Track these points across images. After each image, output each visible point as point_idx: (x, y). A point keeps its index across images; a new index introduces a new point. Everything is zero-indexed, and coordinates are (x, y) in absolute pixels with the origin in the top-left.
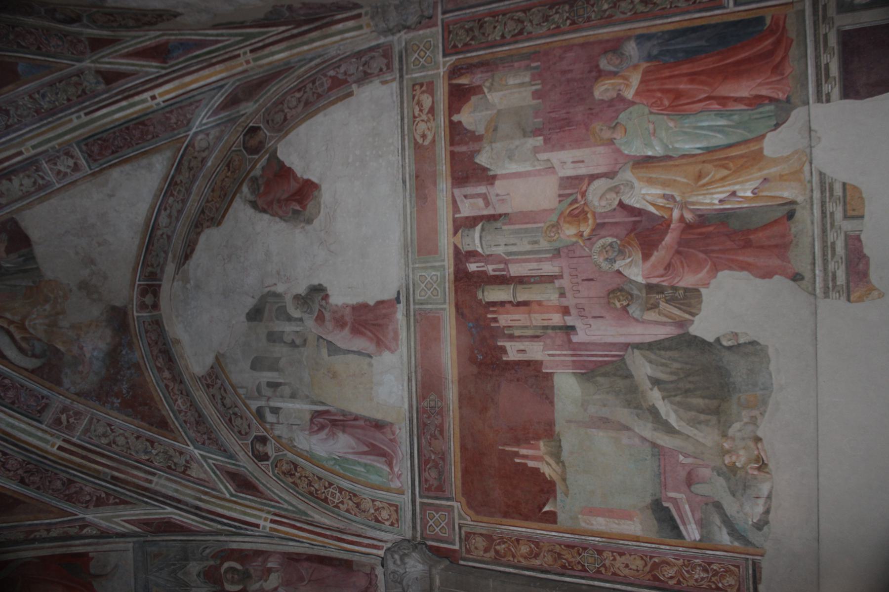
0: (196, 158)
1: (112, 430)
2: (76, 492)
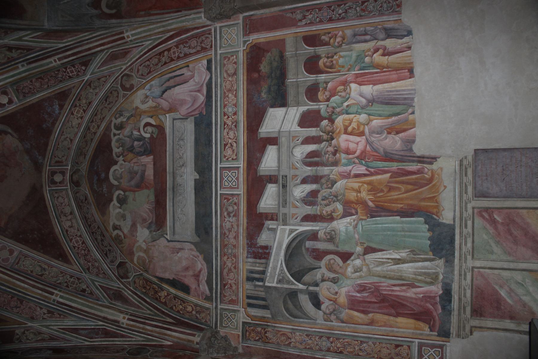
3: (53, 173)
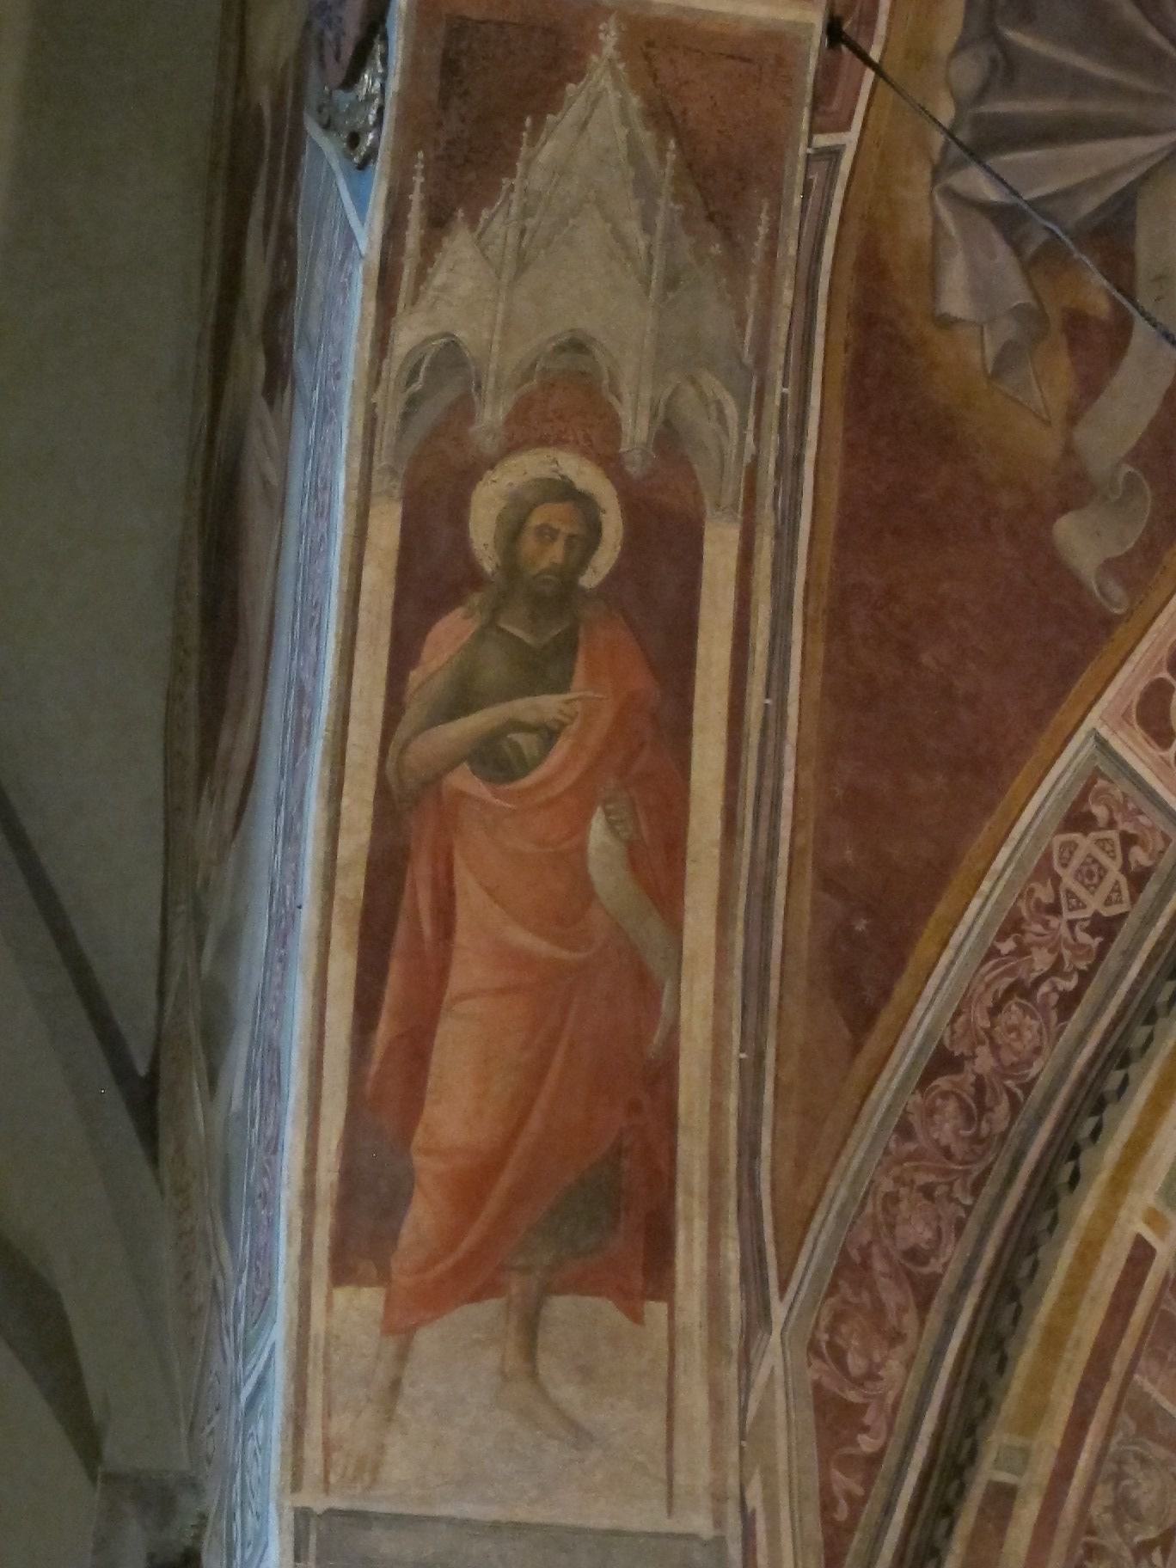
2: (879, 1308)
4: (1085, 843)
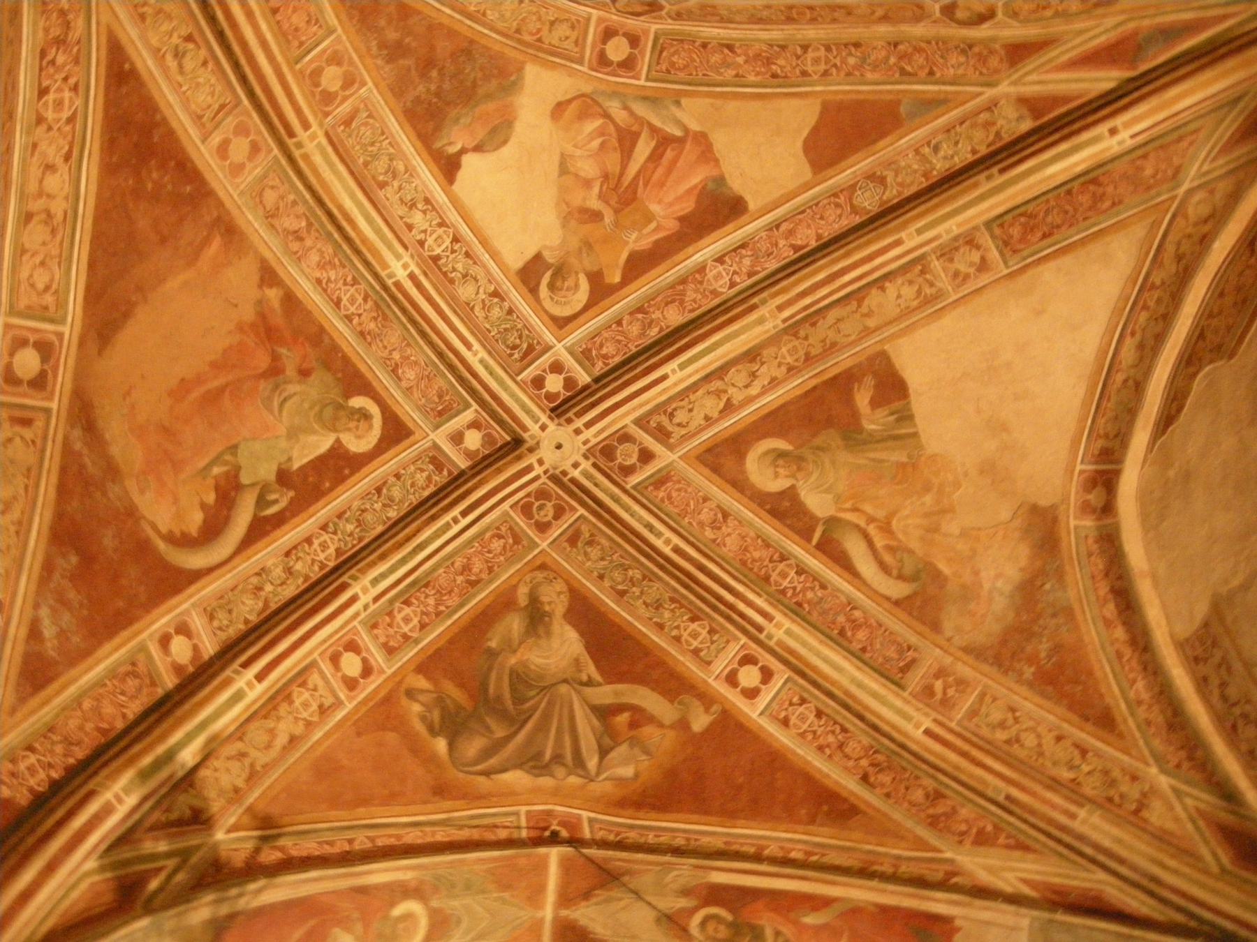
0: (1190, 236)
1: (1016, 720)
2: (945, 814)
3: (39, 383)
4: (793, 720)
